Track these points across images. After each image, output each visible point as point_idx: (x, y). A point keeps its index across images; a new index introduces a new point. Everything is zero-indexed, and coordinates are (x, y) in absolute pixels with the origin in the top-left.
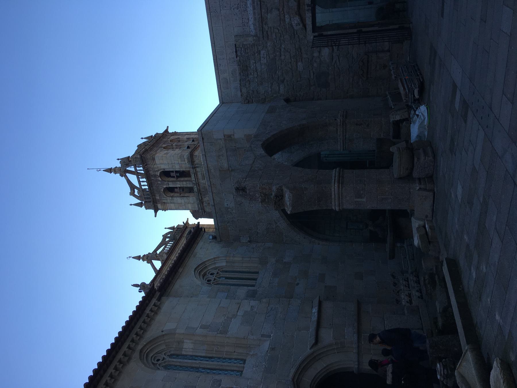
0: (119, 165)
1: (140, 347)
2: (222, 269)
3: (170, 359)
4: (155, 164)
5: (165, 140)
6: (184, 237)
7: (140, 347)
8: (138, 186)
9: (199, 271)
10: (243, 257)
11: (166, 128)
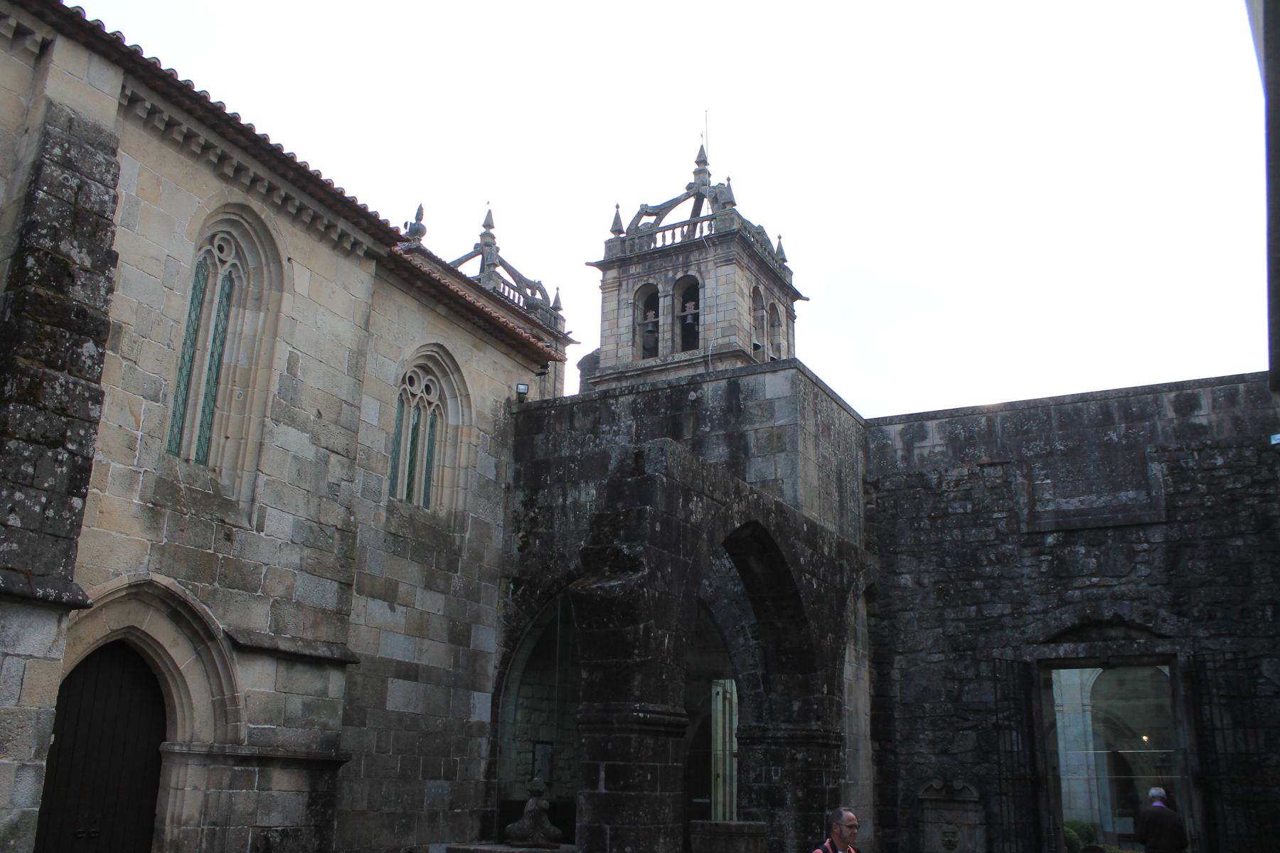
0: (714, 182)
1: (256, 204)
2: (441, 414)
3: (220, 278)
4: (715, 263)
5: (776, 290)
7: (256, 204)
8: (662, 225)
9: (437, 355)
10: (467, 468)
11: (804, 294)
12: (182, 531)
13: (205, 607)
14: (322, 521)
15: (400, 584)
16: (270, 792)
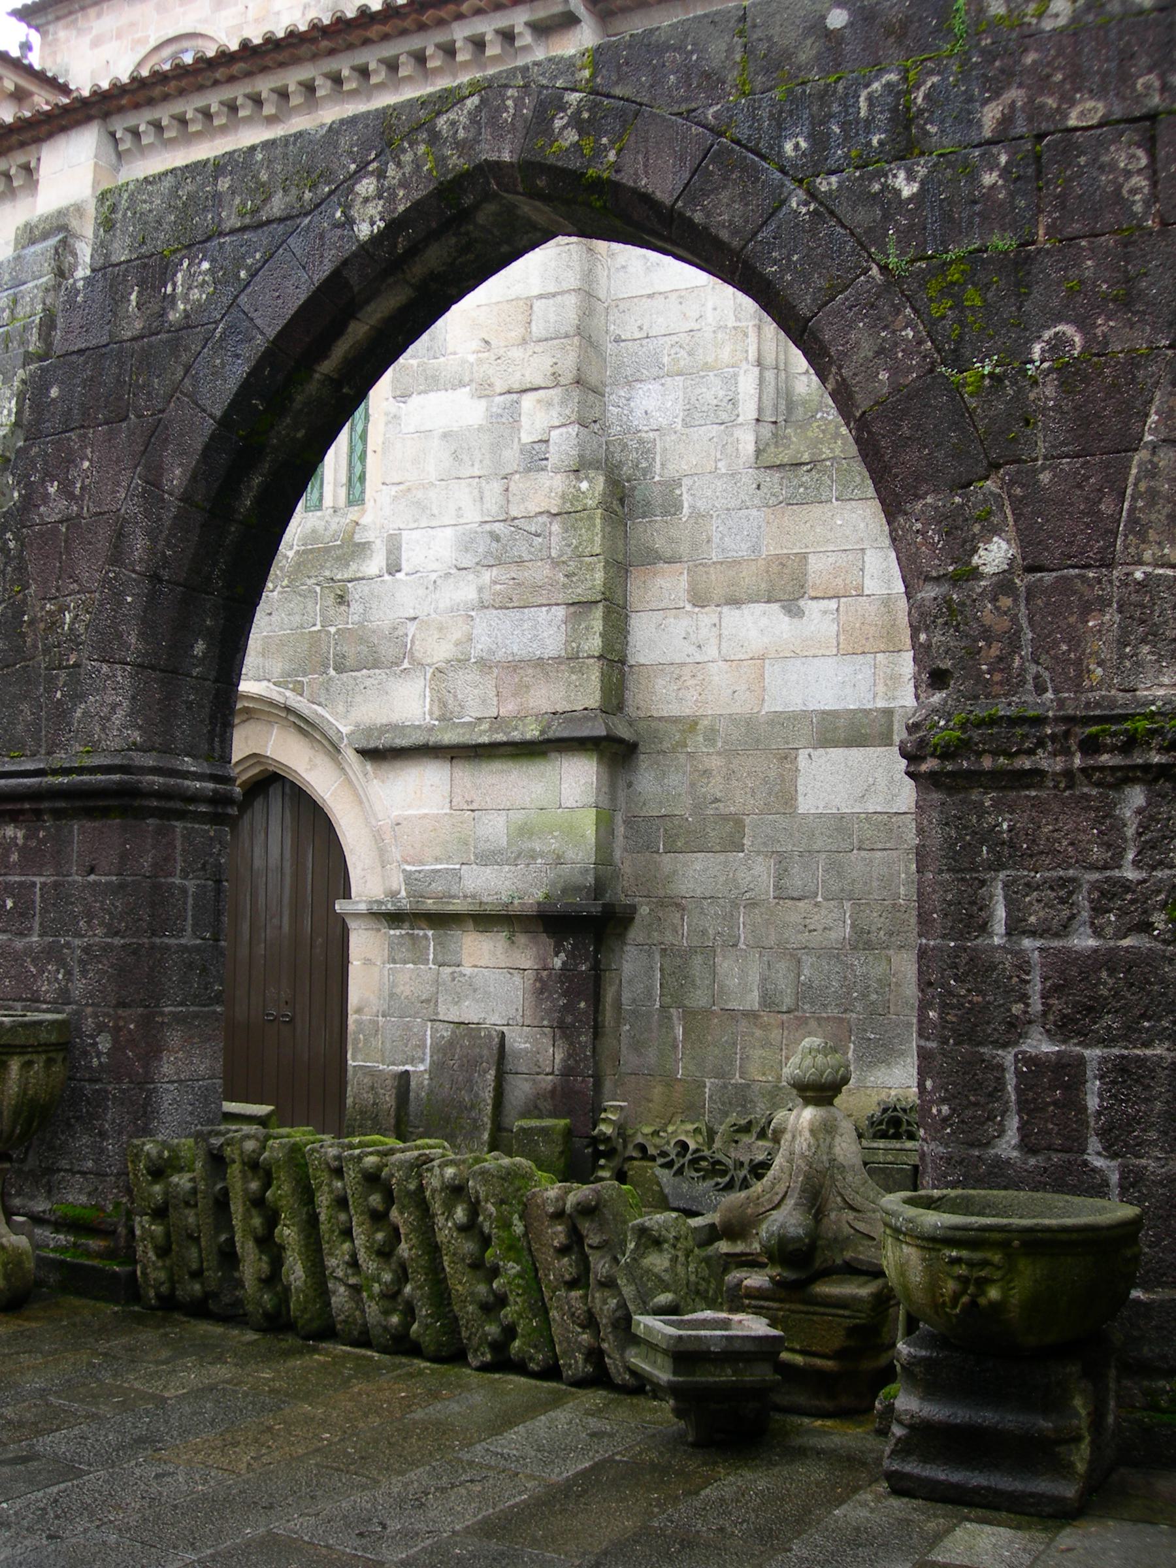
12: (270, 614)
13: (315, 707)
14: (514, 513)
15: (812, 559)
16: (457, 969)
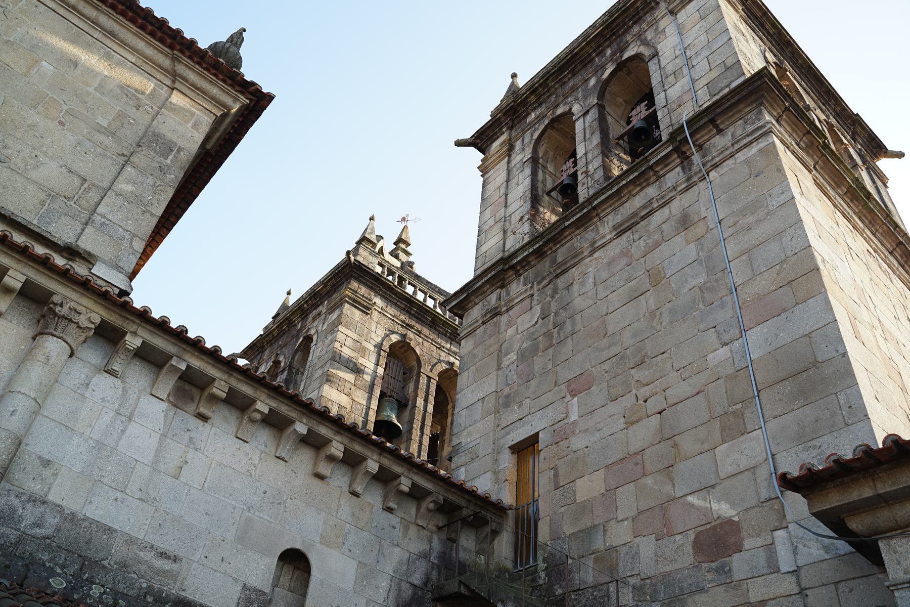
6: (174, 59)
11: (890, 147)
